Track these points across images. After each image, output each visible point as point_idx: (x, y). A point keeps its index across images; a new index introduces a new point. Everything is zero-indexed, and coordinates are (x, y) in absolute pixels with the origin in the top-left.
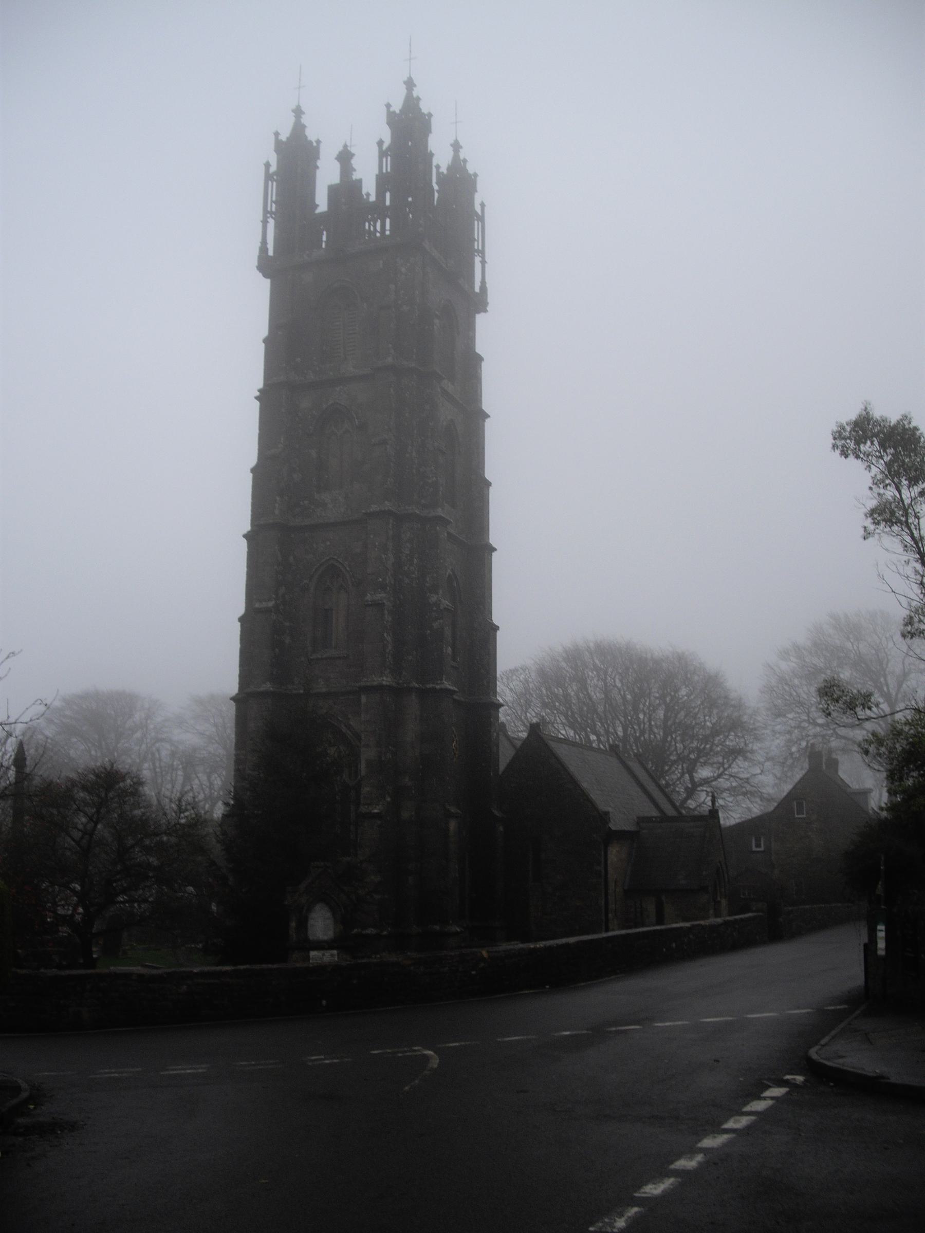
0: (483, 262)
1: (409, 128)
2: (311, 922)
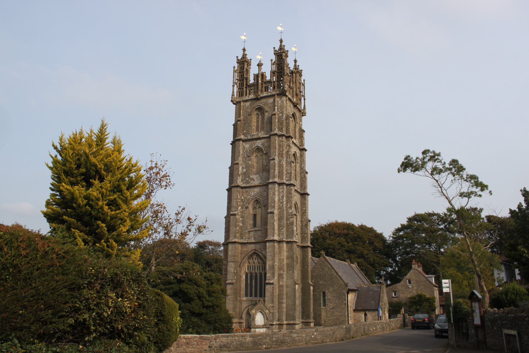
0: (305, 99)
2: (256, 319)
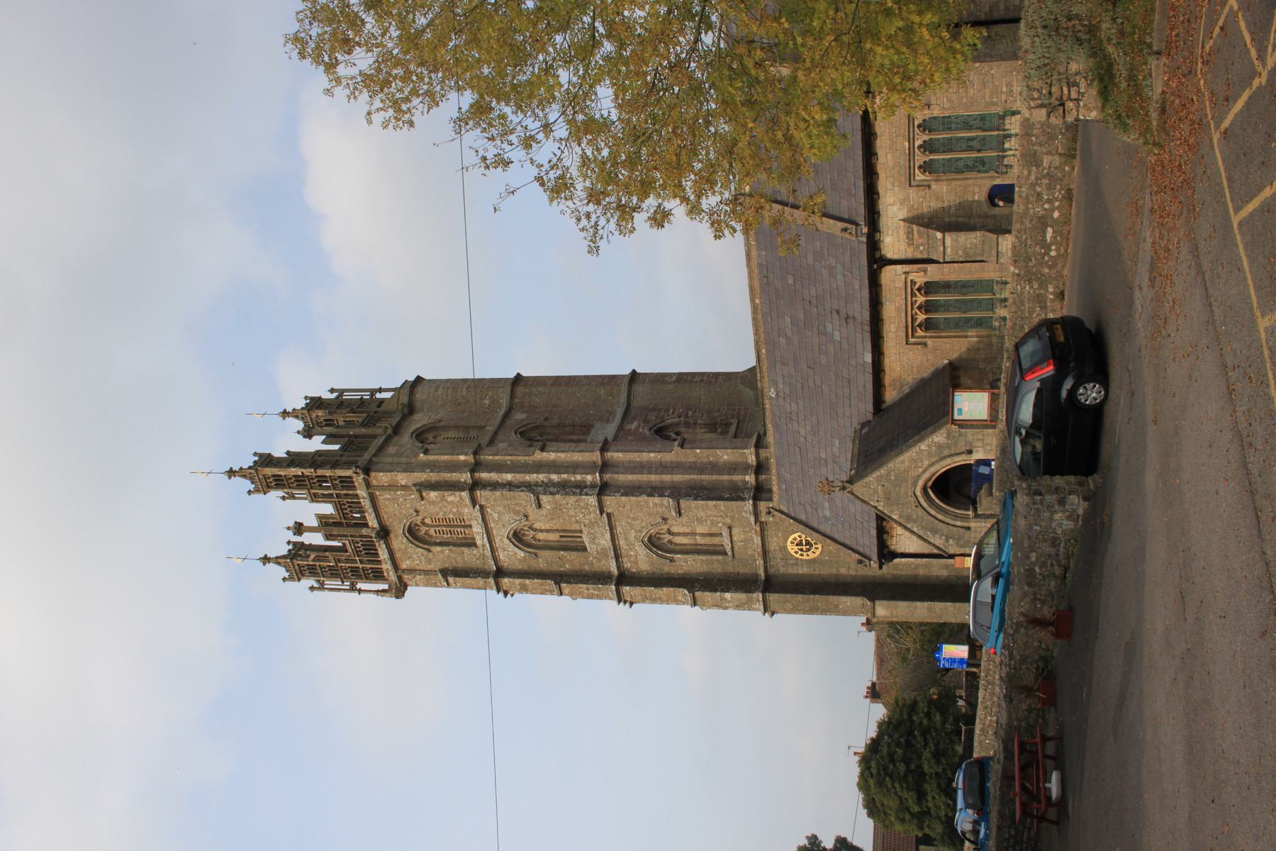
0: (380, 390)
1: (269, 473)
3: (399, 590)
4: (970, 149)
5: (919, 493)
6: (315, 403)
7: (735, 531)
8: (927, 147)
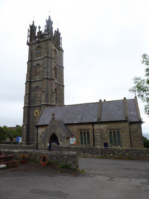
1: (49, 23)
3: (28, 44)
4: (114, 139)
5: (52, 132)
6: (60, 34)
7: (39, 101)
8: (114, 132)
